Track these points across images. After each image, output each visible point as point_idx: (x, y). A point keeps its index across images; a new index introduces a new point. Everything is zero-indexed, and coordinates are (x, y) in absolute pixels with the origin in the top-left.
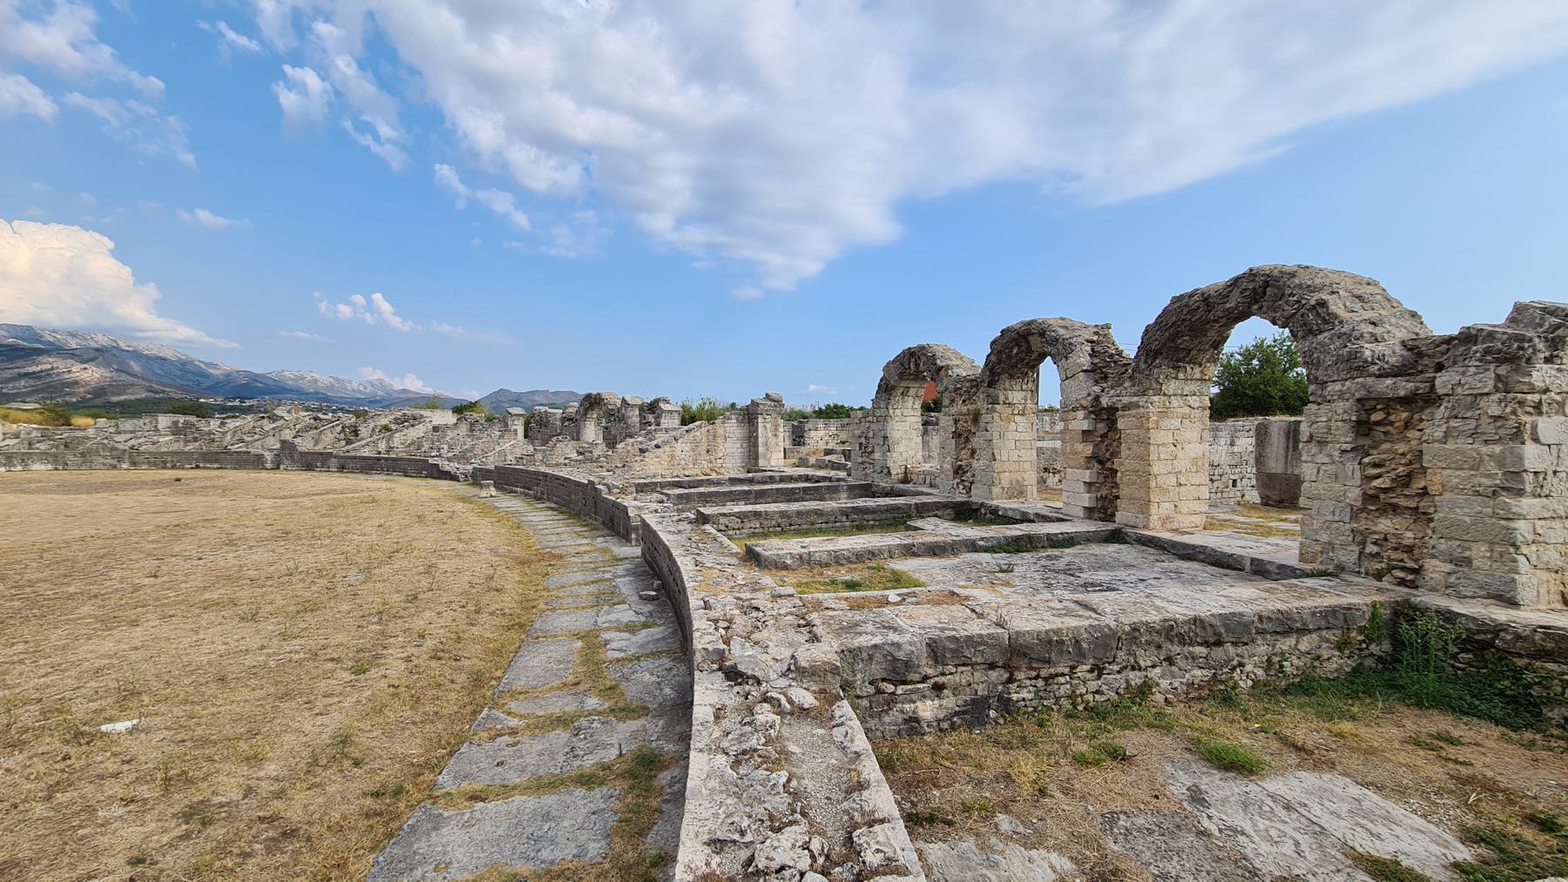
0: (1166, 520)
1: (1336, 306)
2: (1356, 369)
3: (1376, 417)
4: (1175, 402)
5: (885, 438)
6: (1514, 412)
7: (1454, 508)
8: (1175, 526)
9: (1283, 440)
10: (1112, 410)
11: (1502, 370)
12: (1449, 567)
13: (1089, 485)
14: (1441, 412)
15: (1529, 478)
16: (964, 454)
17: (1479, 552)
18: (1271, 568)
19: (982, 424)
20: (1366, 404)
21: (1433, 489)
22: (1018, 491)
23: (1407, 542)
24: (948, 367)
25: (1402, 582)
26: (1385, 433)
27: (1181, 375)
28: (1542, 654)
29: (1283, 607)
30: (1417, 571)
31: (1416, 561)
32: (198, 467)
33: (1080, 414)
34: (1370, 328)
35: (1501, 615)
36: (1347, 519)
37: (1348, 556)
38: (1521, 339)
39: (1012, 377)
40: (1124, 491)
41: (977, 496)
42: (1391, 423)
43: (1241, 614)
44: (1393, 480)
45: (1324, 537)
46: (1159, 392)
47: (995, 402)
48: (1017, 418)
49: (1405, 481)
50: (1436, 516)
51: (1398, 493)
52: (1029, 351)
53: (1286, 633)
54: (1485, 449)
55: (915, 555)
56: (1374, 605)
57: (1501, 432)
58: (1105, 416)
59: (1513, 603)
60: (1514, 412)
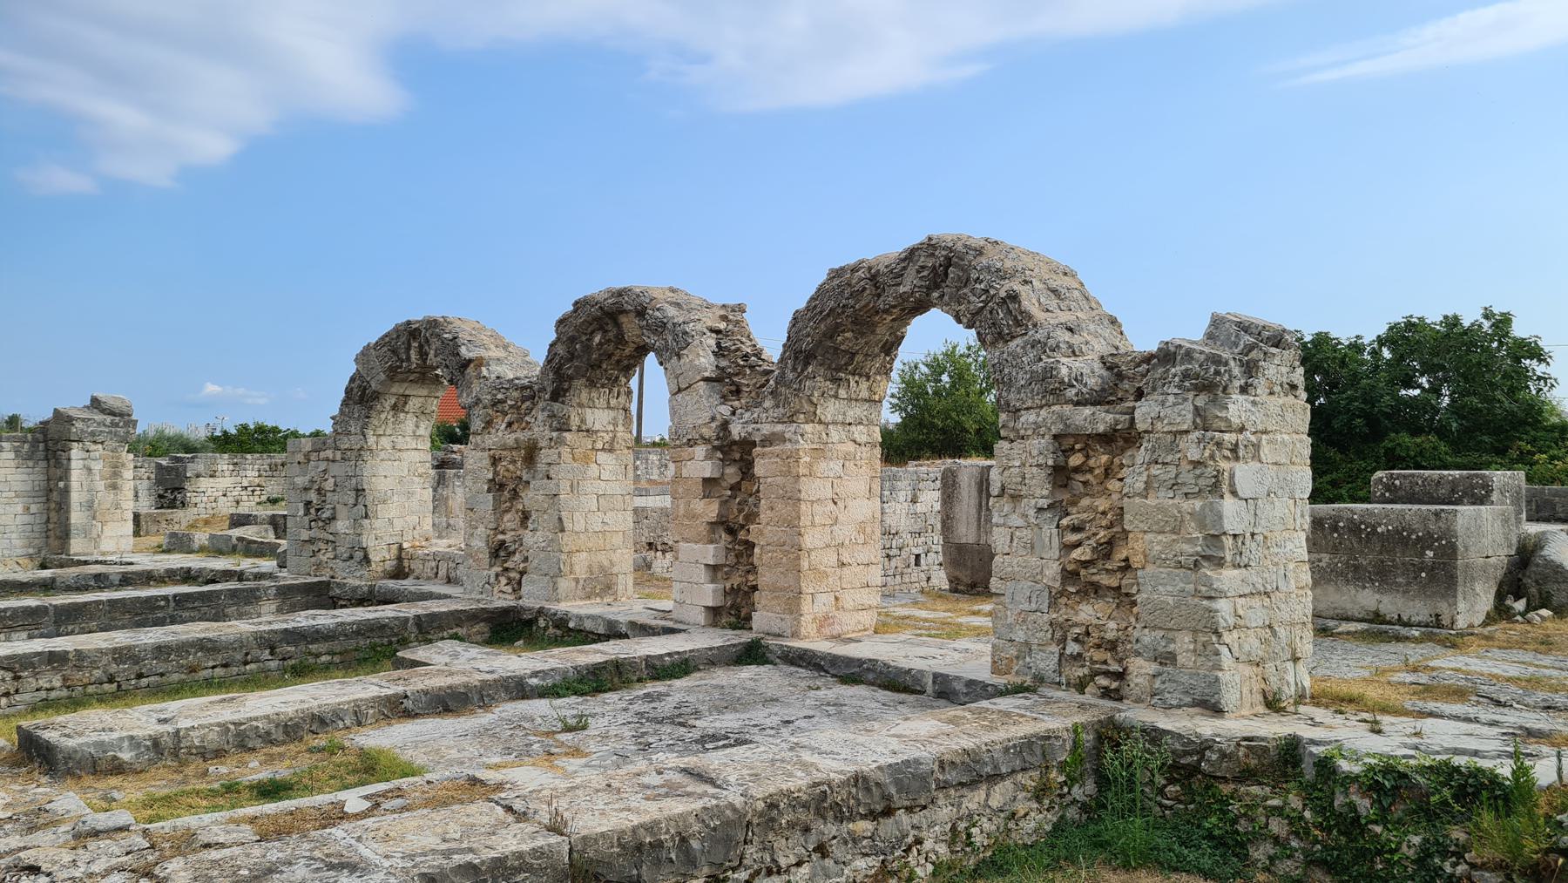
0: (824, 621)
1: (1029, 302)
2: (1053, 392)
3: (1075, 460)
4: (835, 434)
5: (359, 491)
6: (1212, 457)
7: (1158, 587)
8: (837, 629)
9: (974, 493)
10: (747, 445)
11: (1201, 401)
12: (1153, 667)
13: (714, 569)
14: (1141, 455)
15: (1228, 542)
17: (1183, 644)
18: (959, 686)
19: (541, 467)
20: (1064, 441)
21: (1136, 561)
22: (602, 584)
23: (1110, 635)
24: (480, 362)
25: (1107, 693)
26: (1085, 483)
27: (842, 393)
29: (968, 743)
30: (1120, 676)
31: (1120, 661)
33: (700, 451)
34: (1067, 336)
35: (1206, 727)
36: (1045, 607)
37: (1045, 661)
38: (1217, 360)
39: (592, 384)
40: (765, 578)
41: (532, 597)
42: (1091, 470)
43: (917, 762)
44: (1094, 550)
45: (1020, 636)
46: (813, 418)
47: (563, 427)
48: (602, 457)
49: (1106, 550)
50: (1139, 598)
51: (1097, 570)
52: (620, 340)
53: (972, 784)
54: (1187, 505)
55: (409, 715)
56: (1075, 726)
57: (1202, 482)
58: (737, 453)
59: (1217, 711)
60: (1212, 457)
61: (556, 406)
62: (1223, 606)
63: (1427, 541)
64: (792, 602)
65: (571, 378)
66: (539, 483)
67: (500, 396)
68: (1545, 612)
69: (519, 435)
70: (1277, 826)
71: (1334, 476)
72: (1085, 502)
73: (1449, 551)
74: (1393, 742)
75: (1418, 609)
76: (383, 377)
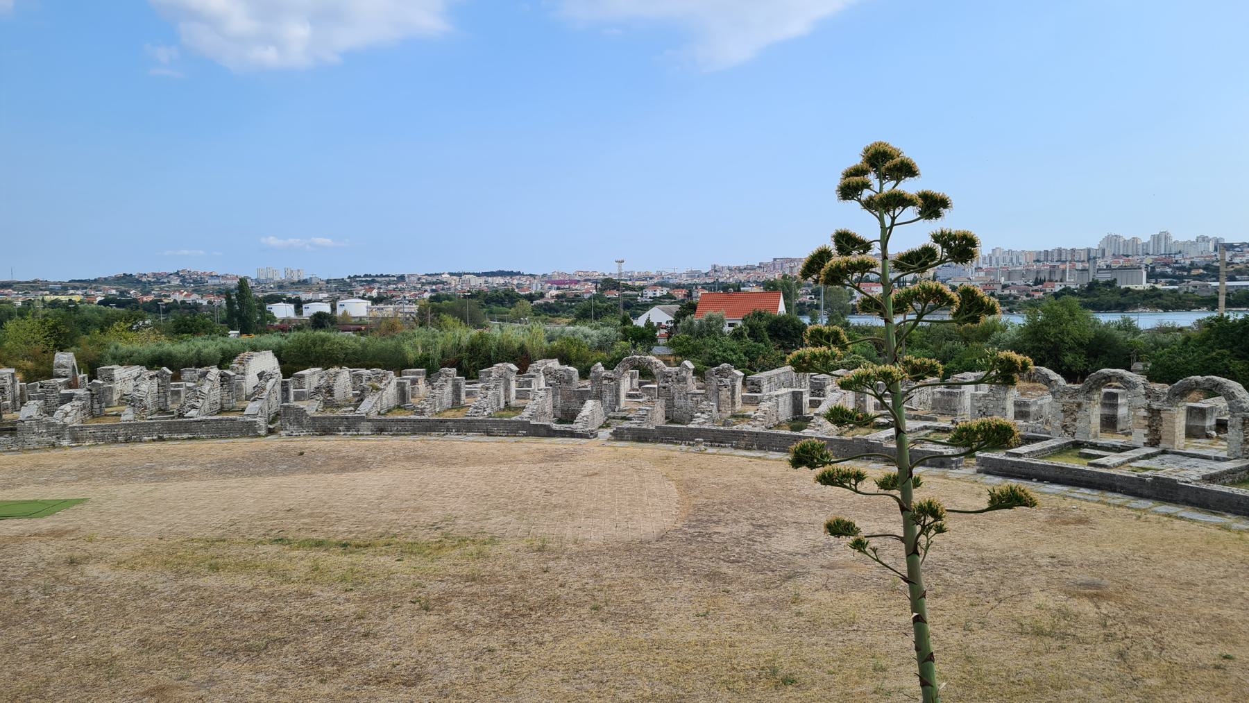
5: (1004, 409)
10: (1159, 411)
32: (161, 439)
37: (1240, 454)
41: (1079, 437)
64: (1173, 443)
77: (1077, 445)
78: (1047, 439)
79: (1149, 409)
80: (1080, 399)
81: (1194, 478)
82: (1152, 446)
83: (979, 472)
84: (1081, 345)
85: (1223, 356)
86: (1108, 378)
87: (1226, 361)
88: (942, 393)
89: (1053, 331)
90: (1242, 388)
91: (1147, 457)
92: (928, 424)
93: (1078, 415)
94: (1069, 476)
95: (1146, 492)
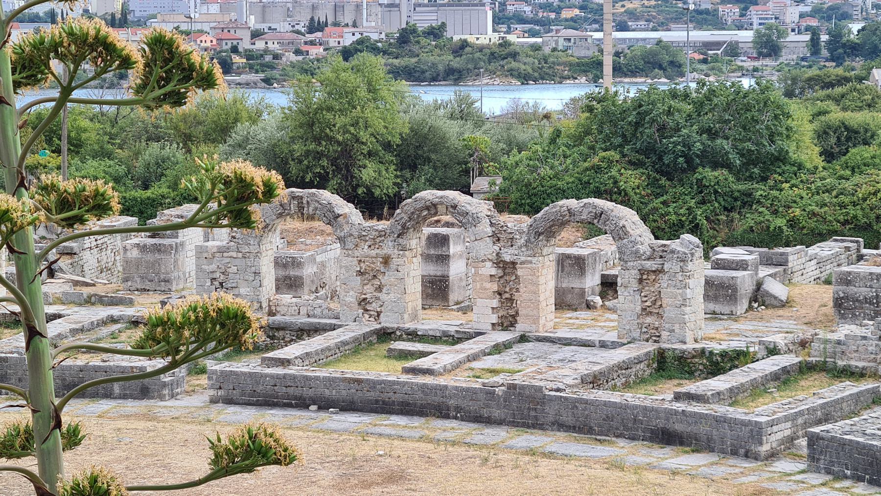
1: (628, 229)
5: (257, 273)
7: (669, 312)
10: (514, 263)
11: (682, 264)
14: (666, 277)
16: (369, 289)
19: (393, 266)
20: (642, 272)
24: (345, 216)
25: (655, 341)
28: (694, 357)
33: (489, 264)
35: (684, 347)
37: (636, 334)
38: (685, 254)
41: (388, 321)
45: (628, 327)
58: (507, 268)
59: (685, 343)
61: (400, 240)
62: (686, 316)
63: (729, 287)
64: (536, 320)
65: (408, 228)
66: (391, 273)
67: (364, 233)
68: (763, 307)
69: (378, 251)
70: (701, 367)
71: (665, 198)
72: (647, 288)
73: (735, 290)
74: (724, 346)
75: (726, 309)
76: (275, 217)
77: (385, 335)
78: (333, 328)
79: (499, 263)
80: (388, 248)
81: (569, 381)
82: (505, 329)
83: (214, 401)
84: (387, 146)
85: (610, 162)
86: (432, 208)
87: (614, 172)
88: (143, 248)
89: (340, 121)
90: (636, 218)
91: (498, 349)
92: (115, 311)
93: (384, 279)
94: (372, 395)
95: (497, 413)
